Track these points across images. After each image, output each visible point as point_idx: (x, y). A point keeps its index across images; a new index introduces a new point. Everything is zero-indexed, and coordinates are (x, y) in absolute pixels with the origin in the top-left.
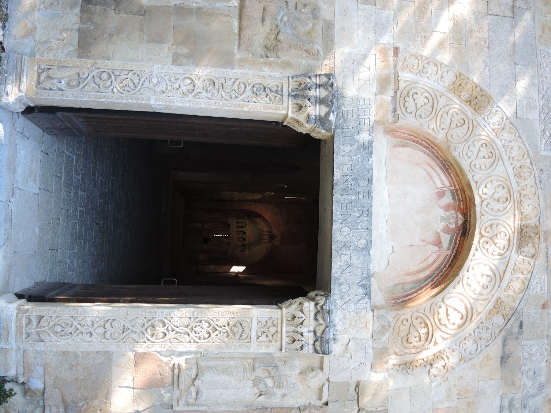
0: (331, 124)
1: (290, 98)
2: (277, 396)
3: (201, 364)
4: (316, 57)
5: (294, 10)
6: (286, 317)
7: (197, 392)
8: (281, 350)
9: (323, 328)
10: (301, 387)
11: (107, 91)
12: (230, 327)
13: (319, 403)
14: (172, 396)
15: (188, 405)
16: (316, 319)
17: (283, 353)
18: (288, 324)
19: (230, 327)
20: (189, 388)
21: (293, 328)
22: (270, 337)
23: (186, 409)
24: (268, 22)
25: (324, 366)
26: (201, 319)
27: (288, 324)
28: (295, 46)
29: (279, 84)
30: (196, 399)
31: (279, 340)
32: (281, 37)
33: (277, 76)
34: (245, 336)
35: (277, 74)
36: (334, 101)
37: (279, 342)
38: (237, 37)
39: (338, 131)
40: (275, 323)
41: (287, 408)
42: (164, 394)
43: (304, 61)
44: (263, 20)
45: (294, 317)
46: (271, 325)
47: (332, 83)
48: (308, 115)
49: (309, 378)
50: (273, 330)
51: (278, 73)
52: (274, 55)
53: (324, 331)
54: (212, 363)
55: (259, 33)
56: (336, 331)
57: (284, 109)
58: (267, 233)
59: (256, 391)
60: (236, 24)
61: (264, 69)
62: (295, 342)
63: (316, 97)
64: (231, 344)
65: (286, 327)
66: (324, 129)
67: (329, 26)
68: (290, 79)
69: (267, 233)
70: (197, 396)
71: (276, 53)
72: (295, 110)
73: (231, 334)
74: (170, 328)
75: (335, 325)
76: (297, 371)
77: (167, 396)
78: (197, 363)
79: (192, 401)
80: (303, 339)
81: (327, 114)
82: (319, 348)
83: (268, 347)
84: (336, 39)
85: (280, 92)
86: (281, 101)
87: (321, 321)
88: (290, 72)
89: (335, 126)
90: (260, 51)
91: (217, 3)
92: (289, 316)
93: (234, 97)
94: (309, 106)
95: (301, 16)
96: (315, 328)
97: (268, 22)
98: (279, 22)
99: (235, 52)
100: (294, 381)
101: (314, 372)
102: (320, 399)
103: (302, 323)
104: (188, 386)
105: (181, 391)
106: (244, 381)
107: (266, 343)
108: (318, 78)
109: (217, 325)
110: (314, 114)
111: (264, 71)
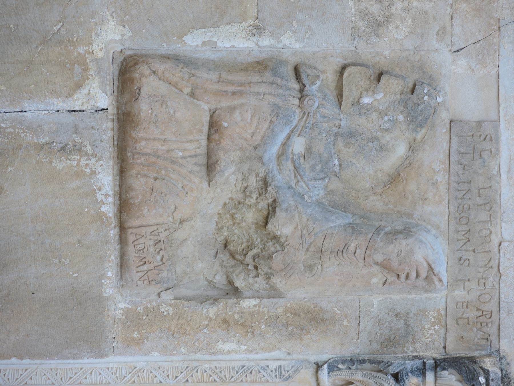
4: (421, 282)
5: (330, 109)
24: (231, 169)
28: (340, 252)
32: (283, 226)
33: (273, 365)
38: (113, 232)
44: (210, 167)
51: (275, 354)
52: (260, 283)
55: (195, 211)
60: (106, 180)
61: (221, 346)
67: (475, 142)
71: (268, 277)
88: (325, 347)
90: (203, 268)
91: (27, 105)
95: (362, 120)
97: (231, 169)
98: (273, 165)
99: (109, 290)
108: (430, 376)
111: (221, 352)
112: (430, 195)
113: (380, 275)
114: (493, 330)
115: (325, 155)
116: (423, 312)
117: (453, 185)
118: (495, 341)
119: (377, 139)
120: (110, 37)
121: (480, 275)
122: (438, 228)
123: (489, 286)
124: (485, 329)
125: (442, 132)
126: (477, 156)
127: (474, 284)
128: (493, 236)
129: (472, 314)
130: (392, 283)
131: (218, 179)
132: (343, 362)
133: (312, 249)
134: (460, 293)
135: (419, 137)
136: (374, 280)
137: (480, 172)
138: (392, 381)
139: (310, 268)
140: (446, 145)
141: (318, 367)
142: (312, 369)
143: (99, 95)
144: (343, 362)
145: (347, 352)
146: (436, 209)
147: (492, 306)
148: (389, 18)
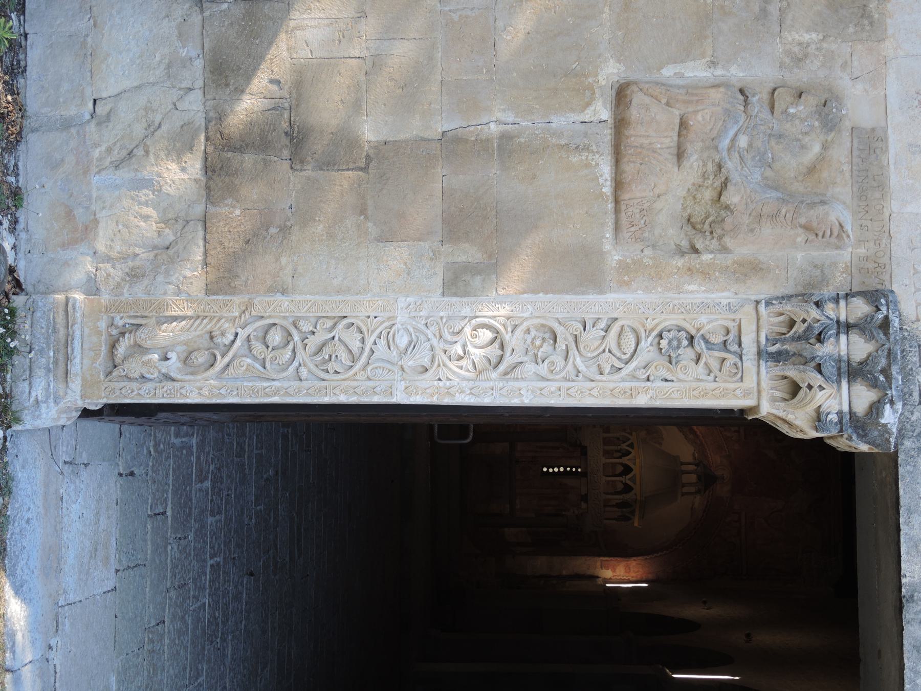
0: (890, 434)
1: (761, 362)
4: (833, 240)
5: (765, 114)
11: (285, 374)
24: (695, 157)
28: (773, 217)
29: (731, 325)
32: (732, 197)
35: (724, 297)
36: (895, 370)
38: (610, 206)
39: (908, 444)
43: (800, 255)
44: (680, 155)
47: (887, 318)
48: (818, 410)
51: (726, 294)
52: (715, 244)
55: (669, 189)
57: (746, 394)
58: (692, 467)
60: (606, 170)
61: (687, 287)
63: (839, 360)
66: (867, 443)
67: (870, 144)
68: (762, 307)
69: (692, 467)
71: (720, 238)
72: (779, 394)
81: (875, 409)
84: (895, 179)
85: (734, 348)
86: (739, 374)
88: (763, 289)
89: (900, 431)
90: (675, 235)
91: (553, 118)
93: (607, 370)
94: (821, 388)
95: (788, 125)
97: (695, 157)
98: (725, 154)
99: (607, 247)
108: (842, 303)
110: (836, 408)
111: (687, 292)
112: (838, 180)
113: (803, 236)
114: (887, 277)
115: (762, 149)
116: (834, 264)
117: (855, 173)
118: (887, 283)
119: (798, 140)
120: (611, 71)
121: (876, 238)
122: (844, 203)
123: (883, 245)
124: (880, 277)
125: (846, 135)
126: (872, 152)
127: (872, 244)
128: (885, 210)
129: (871, 265)
130: (812, 241)
131: (686, 164)
132: (776, 299)
133: (754, 214)
134: (862, 251)
135: (829, 139)
136: (799, 239)
137: (875, 163)
138: (814, 307)
139: (752, 231)
140: (849, 144)
141: (758, 302)
142: (753, 305)
143: (602, 111)
144: (776, 299)
145: (780, 292)
146: (843, 190)
147: (885, 260)
148: (806, 56)
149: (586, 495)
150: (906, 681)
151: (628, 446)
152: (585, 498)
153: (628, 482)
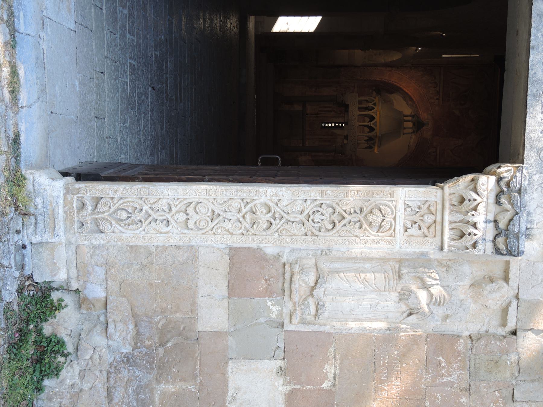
2: (436, 318)
3: (323, 266)
6: (450, 200)
7: (318, 305)
8: (442, 248)
9: (508, 215)
10: (473, 306)
12: (363, 214)
13: (501, 331)
14: (281, 310)
15: (304, 323)
16: (498, 202)
17: (444, 254)
18: (452, 211)
19: (363, 214)
20: (305, 299)
21: (460, 217)
22: (425, 230)
23: (302, 328)
25: (511, 275)
26: (322, 202)
27: (452, 211)
30: (316, 315)
31: (439, 233)
34: (386, 226)
37: (438, 238)
40: (433, 209)
41: (452, 335)
42: (271, 307)
45: (462, 200)
46: (427, 211)
49: (486, 292)
50: (429, 219)
53: (511, 220)
54: (338, 265)
56: (531, 222)
58: (410, 118)
59: (404, 308)
62: (464, 238)
64: (366, 238)
65: (450, 214)
69: (410, 118)
70: (317, 311)
73: (365, 225)
74: (277, 216)
75: (529, 214)
76: (467, 282)
77: (275, 309)
78: (316, 265)
79: (309, 318)
80: (475, 231)
82: (502, 247)
83: (421, 244)
87: (507, 206)
92: (454, 199)
96: (496, 215)
100: (462, 297)
101: (494, 284)
102: (504, 324)
103: (475, 209)
104: (304, 297)
105: (294, 303)
106: (387, 293)
107: (419, 239)
109: (345, 211)
149: (347, 135)
150: (532, 35)
151: (373, 104)
152: (346, 137)
153: (372, 125)
